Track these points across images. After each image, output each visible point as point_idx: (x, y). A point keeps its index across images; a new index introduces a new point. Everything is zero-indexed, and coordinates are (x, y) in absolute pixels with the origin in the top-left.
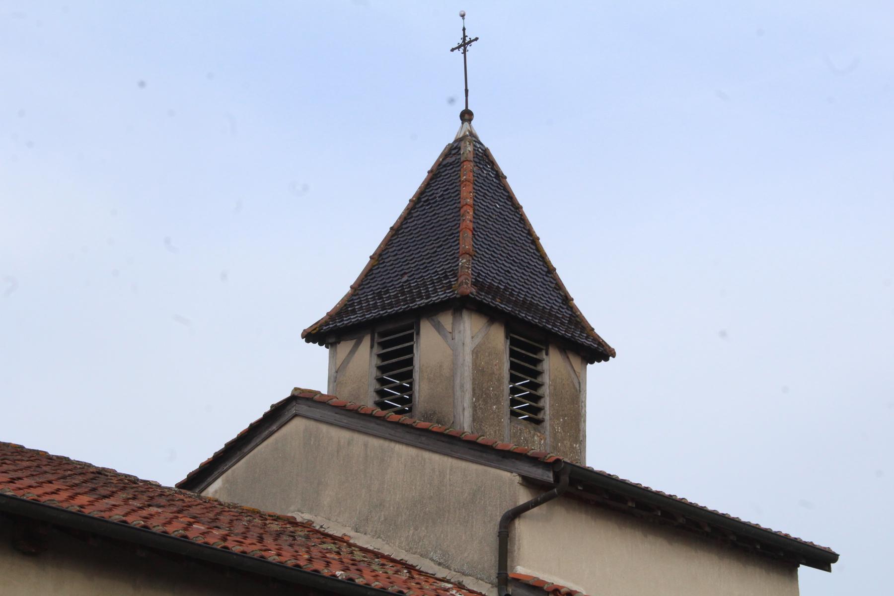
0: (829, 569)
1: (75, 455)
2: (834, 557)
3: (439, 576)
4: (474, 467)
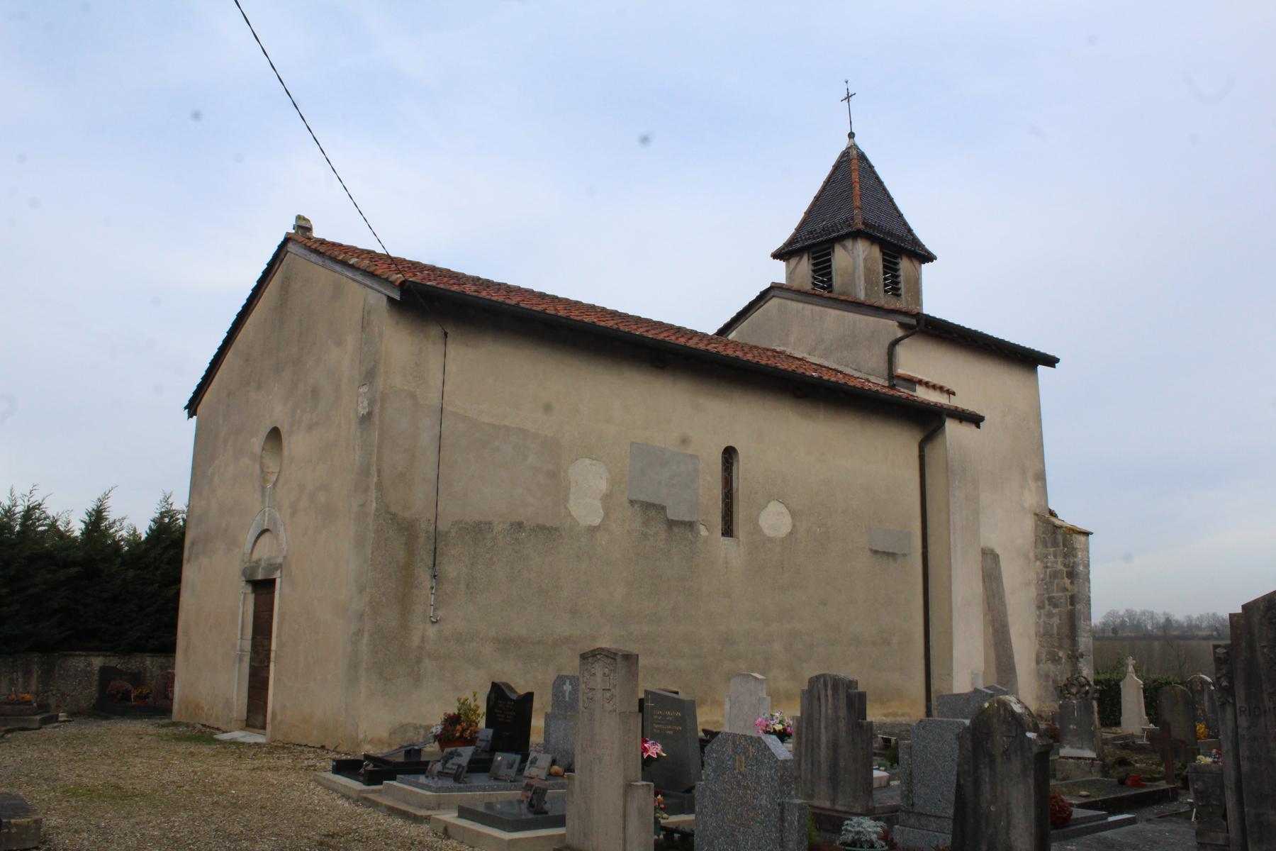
0: (1054, 367)
1: (666, 321)
2: (1057, 360)
3: (855, 376)
4: (872, 319)
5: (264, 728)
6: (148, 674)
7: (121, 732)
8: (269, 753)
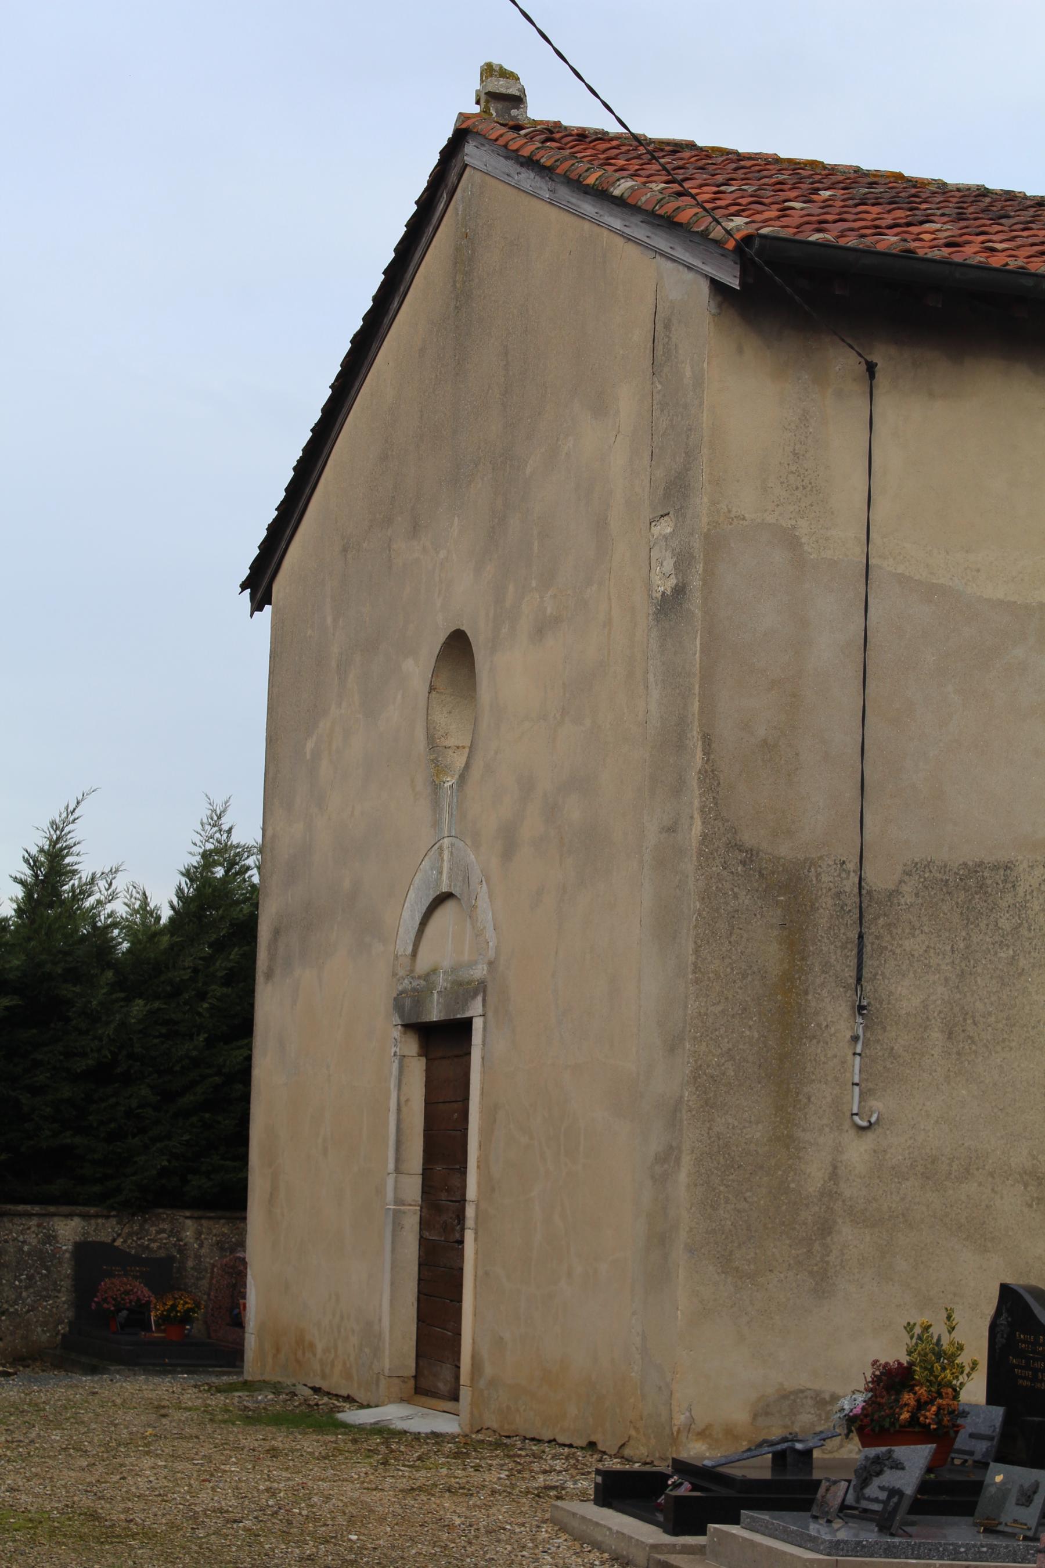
5: (456, 1398)
6: (190, 1263)
7: (119, 1401)
8: (457, 1455)
